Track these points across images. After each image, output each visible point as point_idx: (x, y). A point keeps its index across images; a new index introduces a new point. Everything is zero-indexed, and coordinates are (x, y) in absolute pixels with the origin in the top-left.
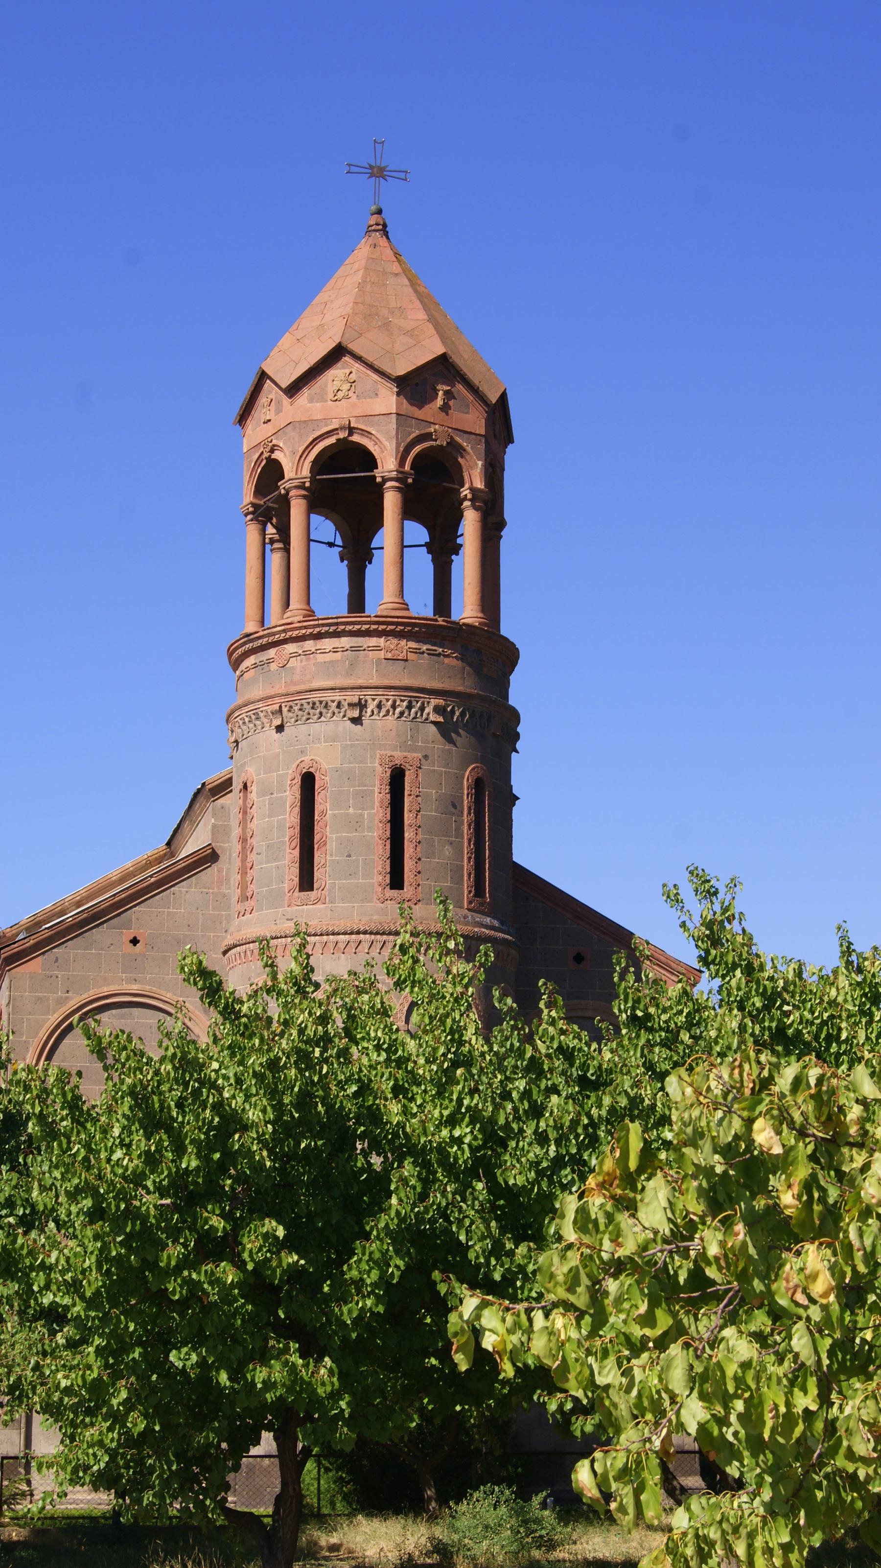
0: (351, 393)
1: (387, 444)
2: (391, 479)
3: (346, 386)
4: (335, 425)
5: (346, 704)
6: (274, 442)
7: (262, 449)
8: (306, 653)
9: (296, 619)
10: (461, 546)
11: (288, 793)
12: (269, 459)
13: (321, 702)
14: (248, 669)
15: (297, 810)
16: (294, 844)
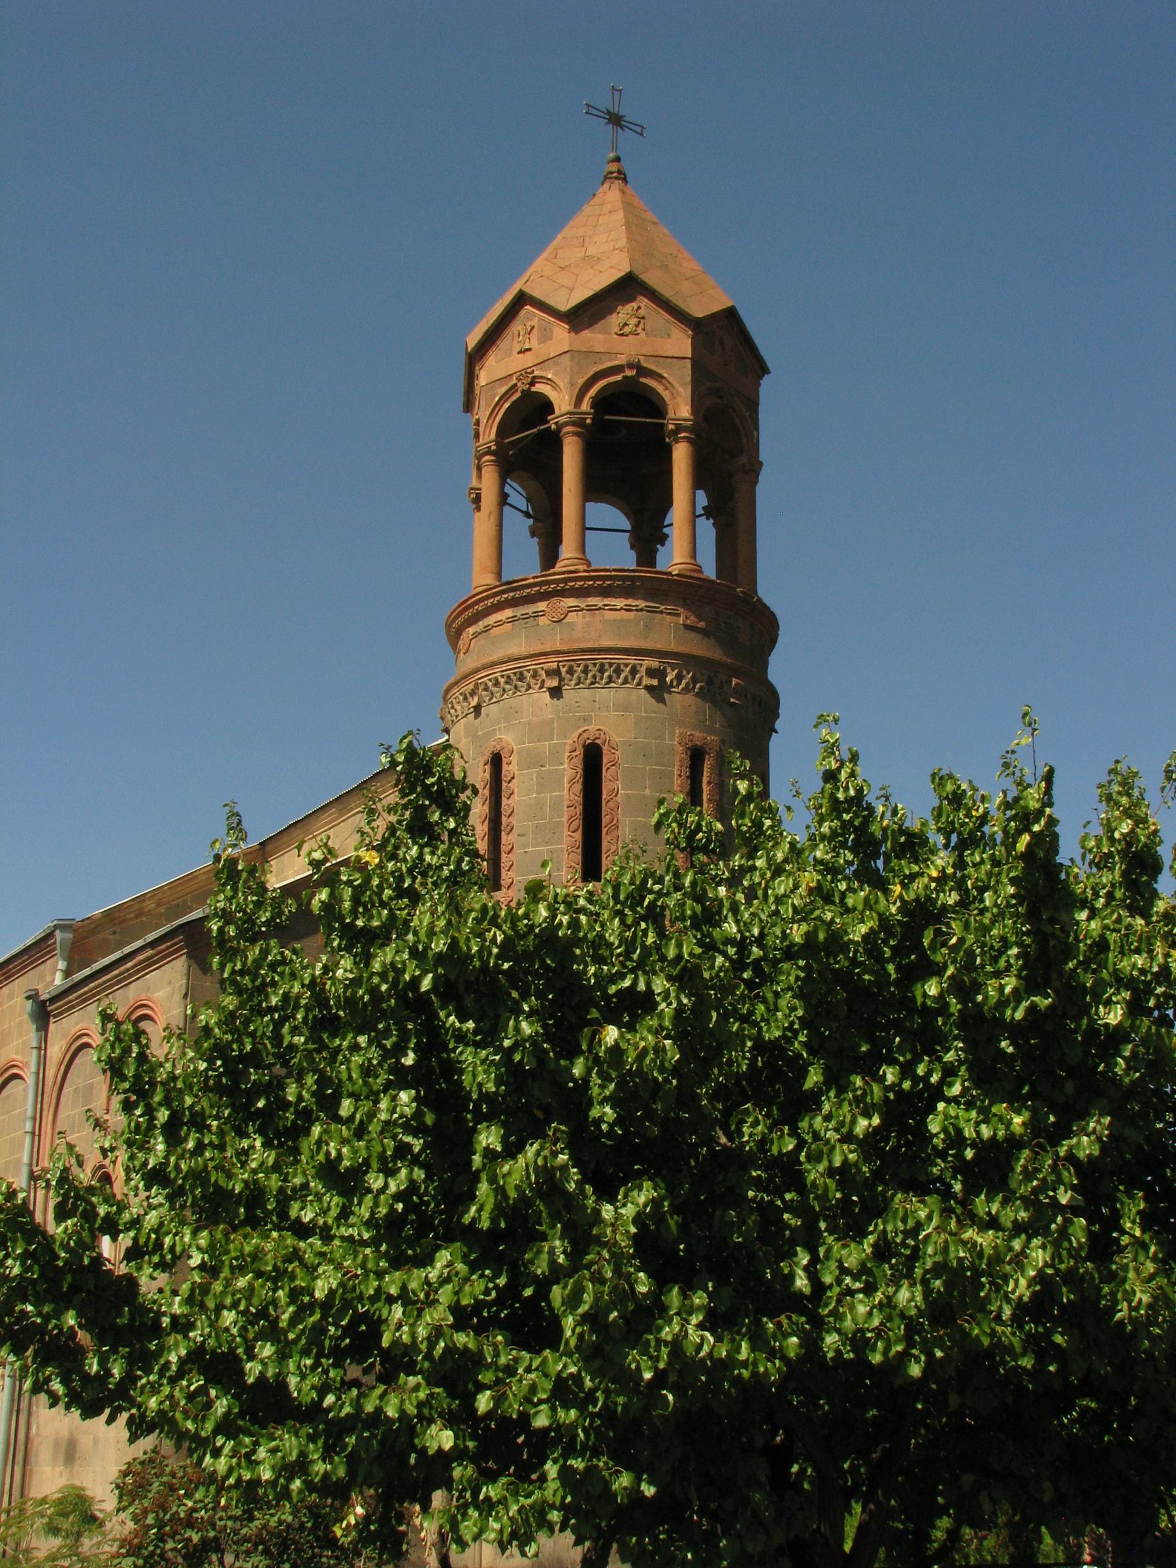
0: (639, 330)
1: (681, 390)
2: (685, 429)
3: (633, 321)
4: (621, 360)
5: (643, 669)
6: (537, 373)
7: (514, 381)
8: (591, 609)
9: (581, 568)
10: (668, 536)
12: (528, 395)
13: (611, 665)
14: (499, 623)
15: (578, 787)
16: (574, 825)
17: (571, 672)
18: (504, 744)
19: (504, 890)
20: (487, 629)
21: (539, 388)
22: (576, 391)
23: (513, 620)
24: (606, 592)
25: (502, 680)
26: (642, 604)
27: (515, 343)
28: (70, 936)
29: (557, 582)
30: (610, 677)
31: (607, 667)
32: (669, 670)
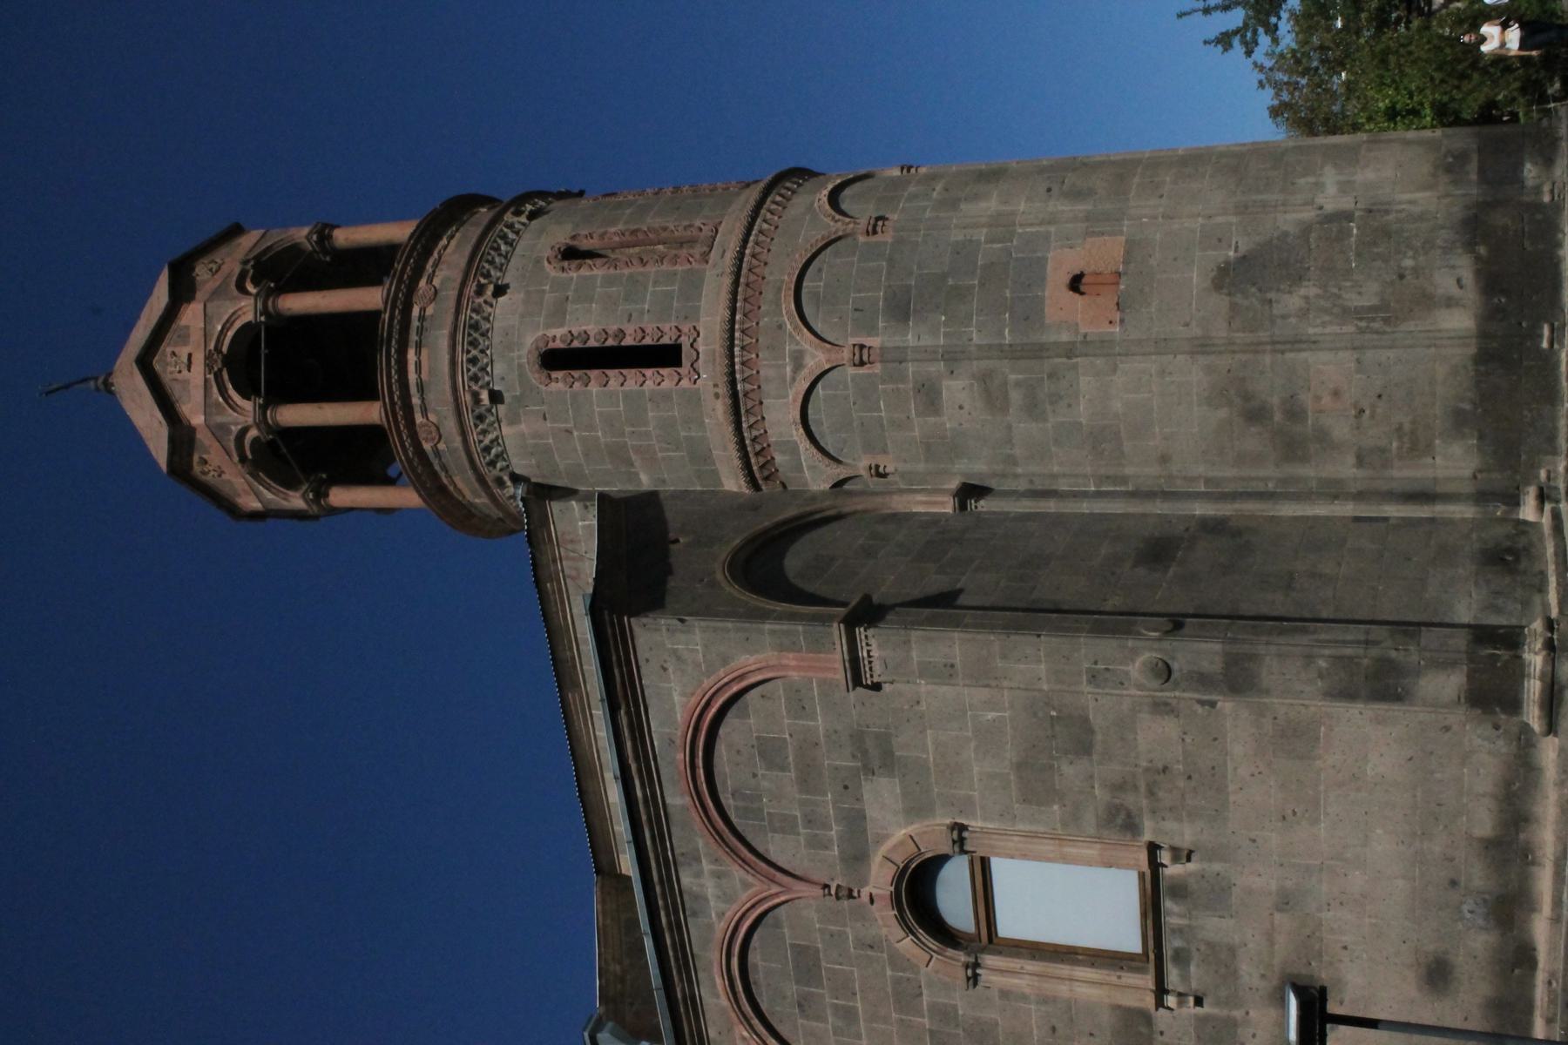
4: (237, 270)
6: (212, 346)
7: (211, 377)
8: (436, 265)
11: (575, 275)
14: (418, 365)
17: (487, 275)
18: (534, 346)
19: (685, 342)
20: (421, 387)
21: (225, 349)
22: (241, 295)
23: (419, 346)
24: (427, 253)
25: (474, 352)
26: (454, 228)
27: (179, 376)
28: (610, 1025)
29: (398, 289)
30: (506, 243)
31: (495, 245)
32: (523, 208)
